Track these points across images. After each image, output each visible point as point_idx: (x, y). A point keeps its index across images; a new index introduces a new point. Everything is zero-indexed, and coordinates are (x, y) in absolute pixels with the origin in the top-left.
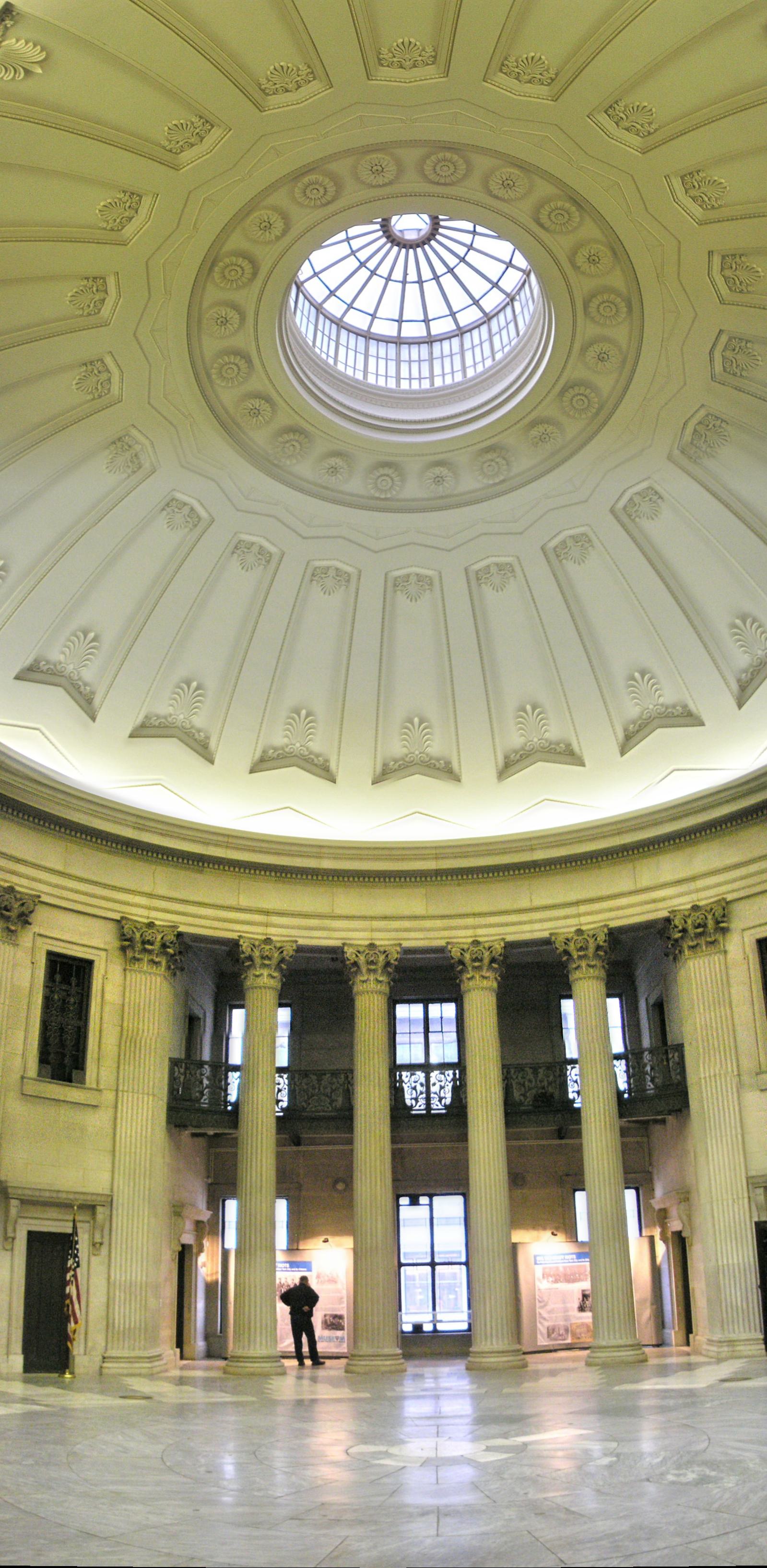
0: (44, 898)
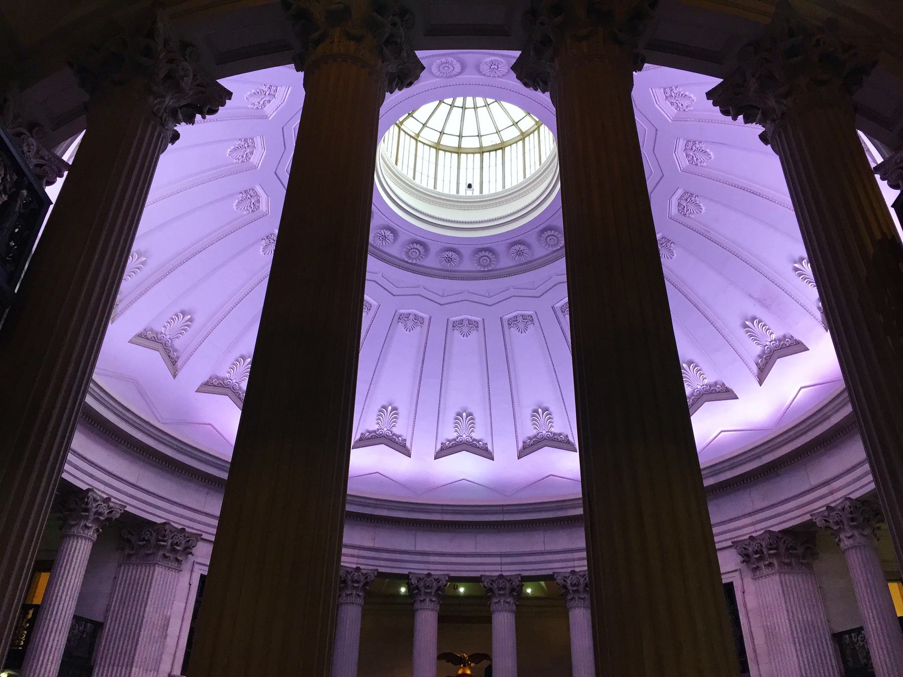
0: (205, 536)
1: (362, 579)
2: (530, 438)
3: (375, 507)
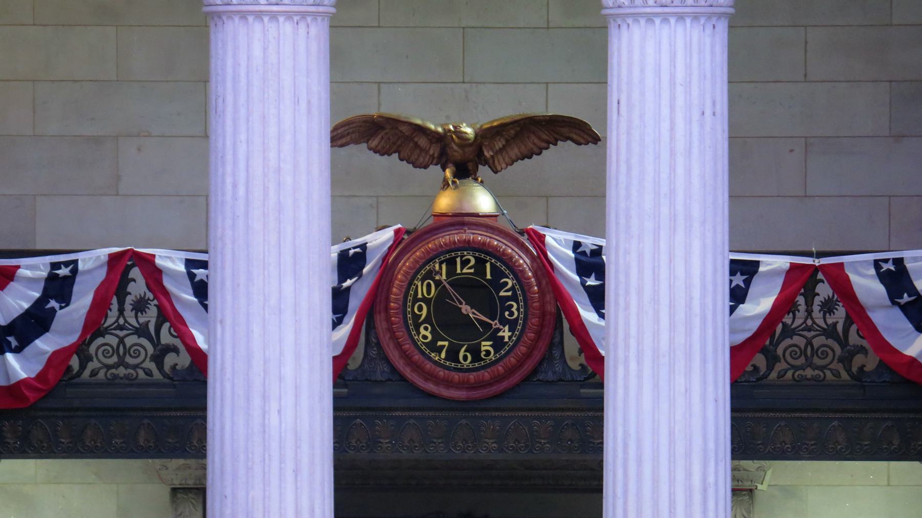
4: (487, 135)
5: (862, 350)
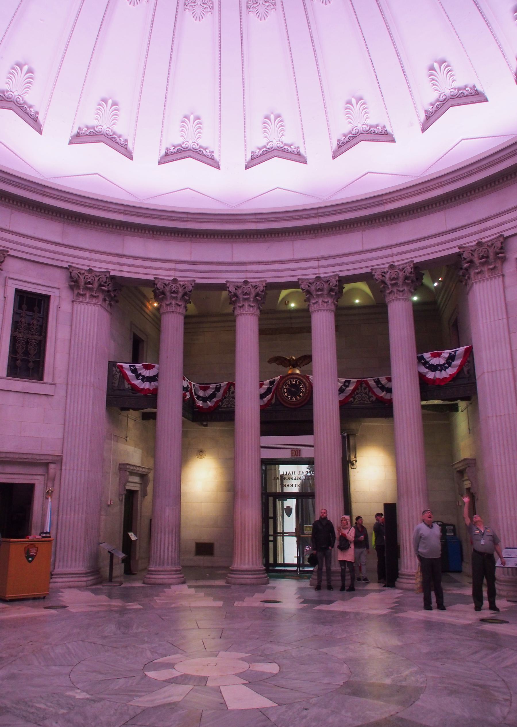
0: (11, 253)
1: (181, 290)
2: (345, 135)
3: (187, 220)
4: (297, 360)
5: (372, 397)
